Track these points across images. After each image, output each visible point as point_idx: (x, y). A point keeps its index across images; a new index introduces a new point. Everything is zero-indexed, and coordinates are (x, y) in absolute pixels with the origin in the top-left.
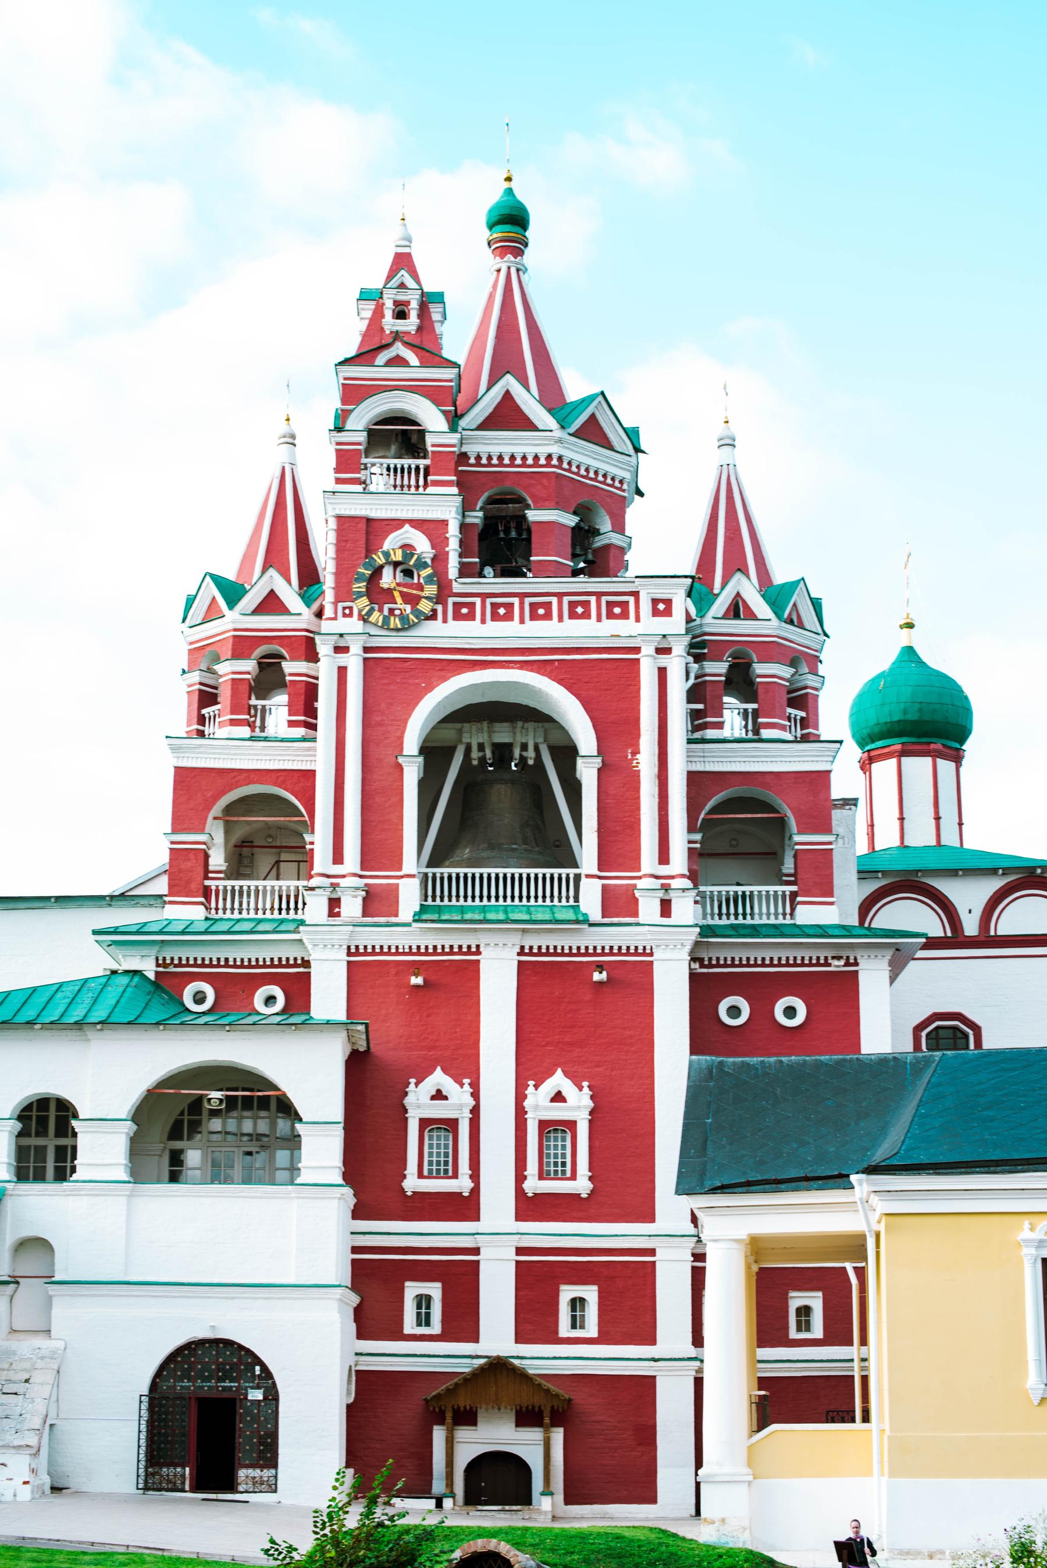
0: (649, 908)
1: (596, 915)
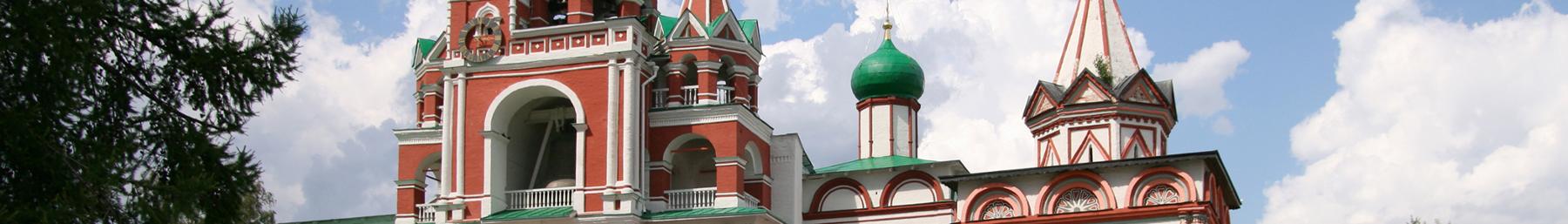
0: (608, 207)
1: (581, 211)
